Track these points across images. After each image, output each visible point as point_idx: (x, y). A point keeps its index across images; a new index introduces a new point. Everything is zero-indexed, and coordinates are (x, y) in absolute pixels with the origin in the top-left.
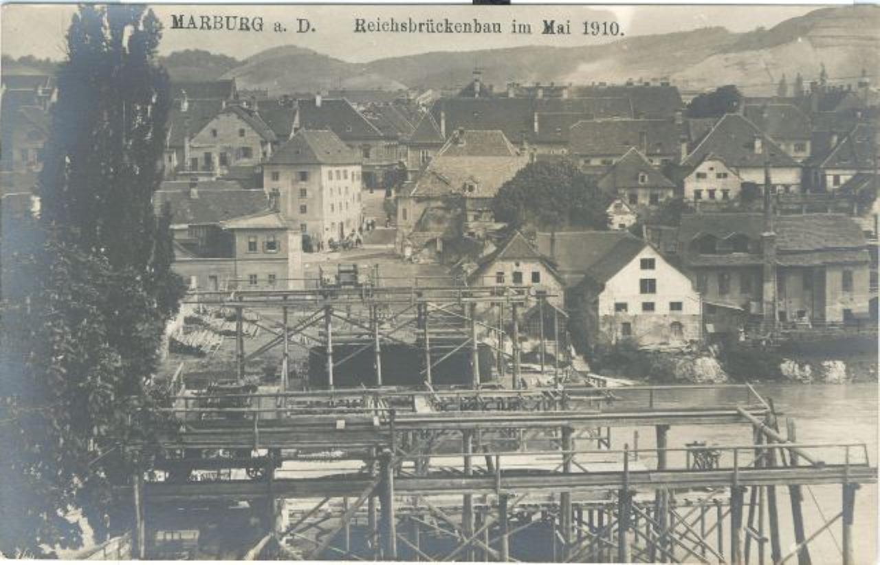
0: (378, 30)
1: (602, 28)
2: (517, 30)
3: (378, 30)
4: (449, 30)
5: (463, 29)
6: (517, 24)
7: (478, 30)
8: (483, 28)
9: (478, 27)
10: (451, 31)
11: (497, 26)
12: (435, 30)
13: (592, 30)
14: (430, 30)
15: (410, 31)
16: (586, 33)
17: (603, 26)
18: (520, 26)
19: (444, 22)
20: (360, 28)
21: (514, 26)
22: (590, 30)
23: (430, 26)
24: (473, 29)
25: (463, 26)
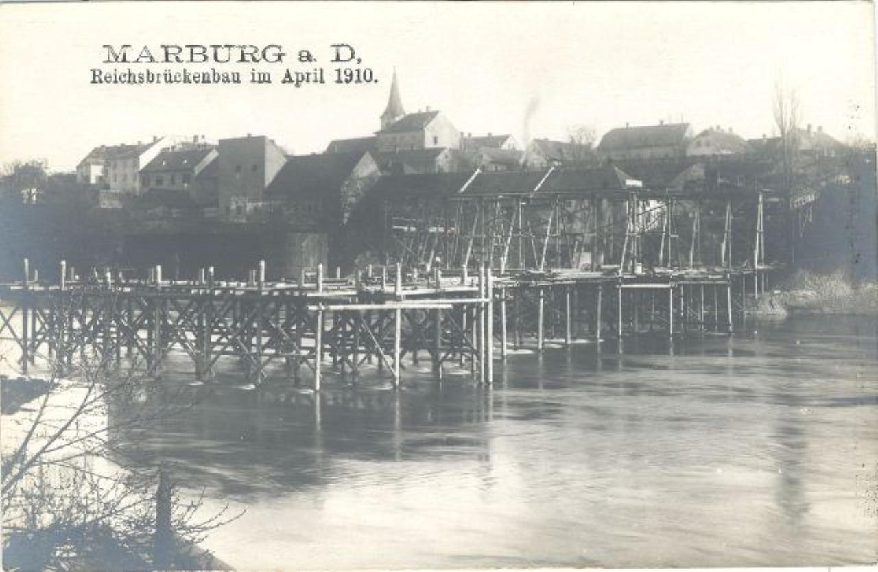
2: (257, 78)
6: (256, 72)
8: (222, 77)
11: (236, 75)
19: (182, 73)
20: (97, 79)
24: (211, 79)
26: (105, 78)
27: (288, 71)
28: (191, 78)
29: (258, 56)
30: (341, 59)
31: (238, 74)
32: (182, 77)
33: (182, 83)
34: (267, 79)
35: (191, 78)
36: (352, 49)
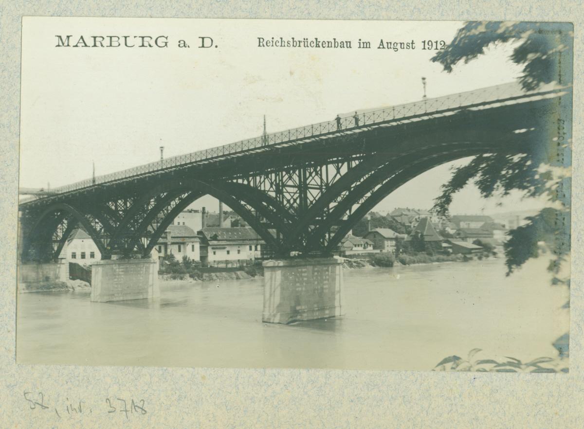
0: (273, 46)
1: (434, 44)
2: (362, 46)
3: (273, 46)
4: (317, 46)
5: (327, 46)
6: (361, 42)
7: (336, 46)
8: (339, 45)
9: (336, 44)
10: (319, 47)
11: (348, 43)
12: (309, 45)
13: (428, 46)
14: (306, 45)
15: (293, 46)
16: (424, 49)
17: (435, 44)
18: (364, 43)
20: (261, 44)
21: (360, 43)
22: (427, 46)
23: (306, 43)
25: (327, 43)
26: (267, 43)
27: (382, 41)
28: (320, 44)
29: (153, 43)
30: (205, 46)
31: (350, 42)
32: (315, 44)
33: (314, 48)
34: (368, 46)
35: (320, 44)
36: (212, 41)
